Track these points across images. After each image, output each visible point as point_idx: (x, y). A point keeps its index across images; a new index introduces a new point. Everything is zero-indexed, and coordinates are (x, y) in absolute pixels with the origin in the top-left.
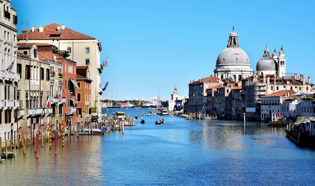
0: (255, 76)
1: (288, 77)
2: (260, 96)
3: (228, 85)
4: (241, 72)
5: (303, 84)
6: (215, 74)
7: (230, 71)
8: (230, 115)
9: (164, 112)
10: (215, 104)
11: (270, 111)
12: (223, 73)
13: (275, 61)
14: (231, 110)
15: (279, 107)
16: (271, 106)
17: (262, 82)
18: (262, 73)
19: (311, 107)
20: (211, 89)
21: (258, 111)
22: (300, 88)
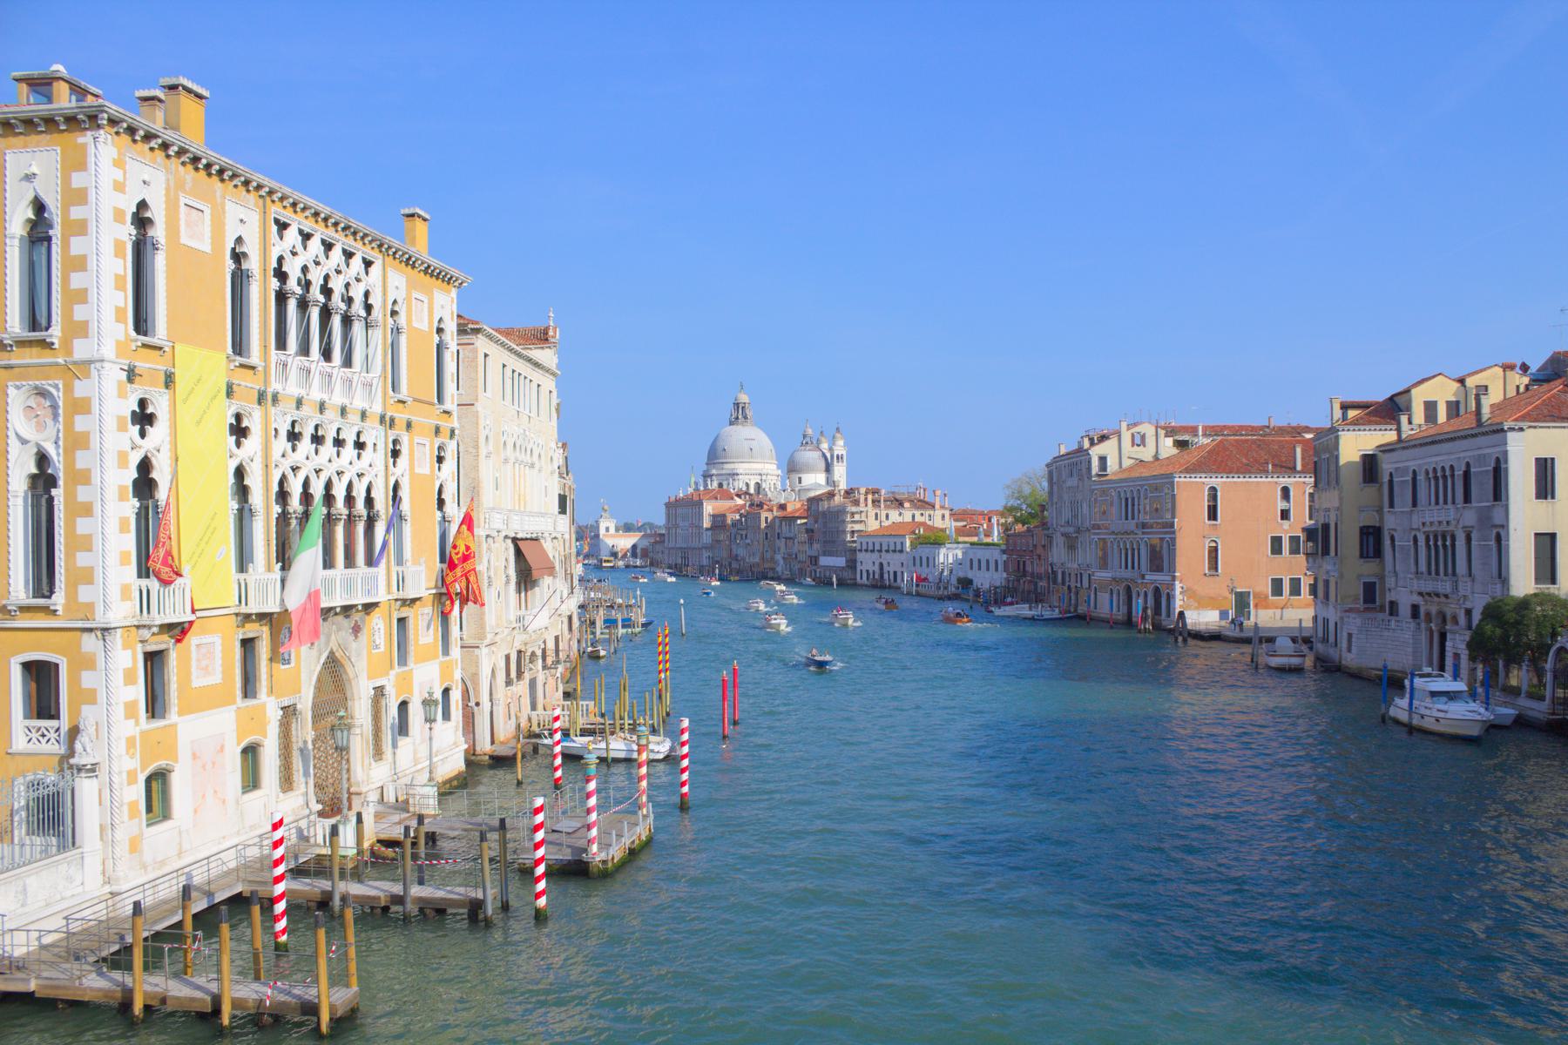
0: (836, 492)
1: (902, 492)
2: (853, 532)
3: (765, 507)
4: (759, 477)
5: (937, 506)
6: (705, 482)
7: (738, 474)
8: (773, 569)
9: (605, 561)
10: (734, 547)
11: (881, 564)
12: (724, 477)
13: (824, 455)
14: (772, 558)
15: (903, 557)
16: (884, 554)
17: (856, 503)
18: (800, 479)
19: (996, 562)
20: (724, 516)
21: (852, 564)
22: (930, 516)
